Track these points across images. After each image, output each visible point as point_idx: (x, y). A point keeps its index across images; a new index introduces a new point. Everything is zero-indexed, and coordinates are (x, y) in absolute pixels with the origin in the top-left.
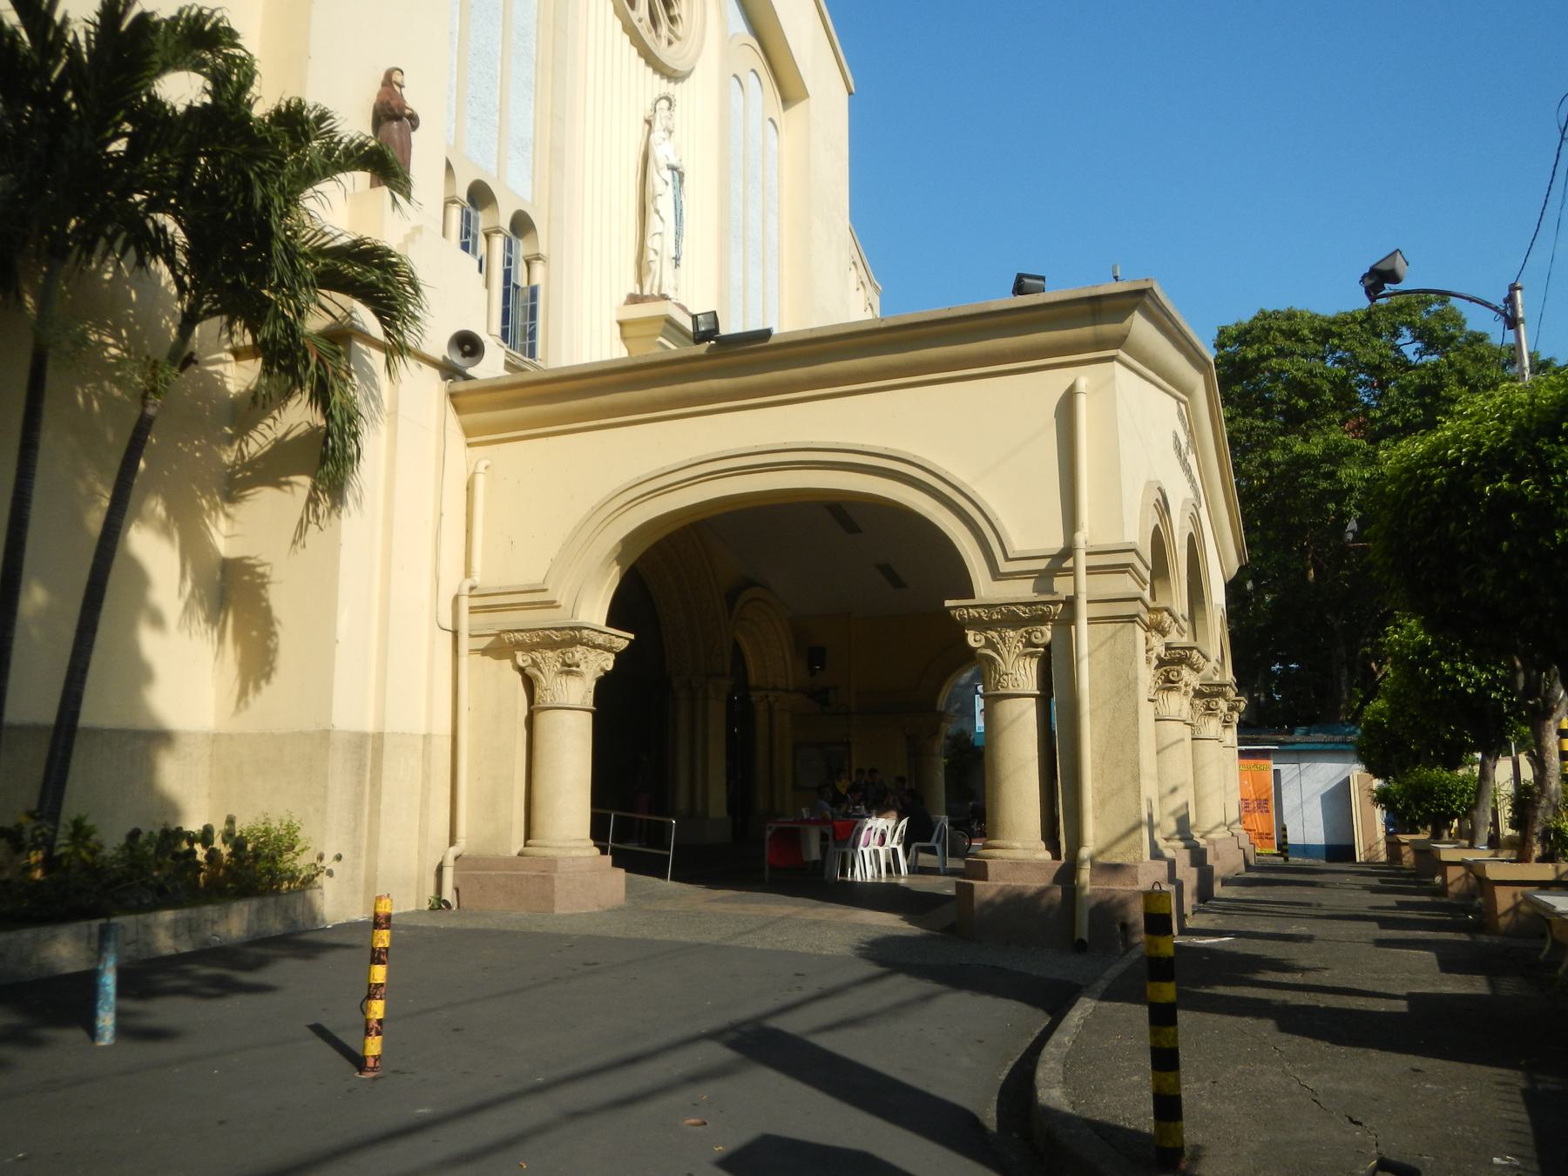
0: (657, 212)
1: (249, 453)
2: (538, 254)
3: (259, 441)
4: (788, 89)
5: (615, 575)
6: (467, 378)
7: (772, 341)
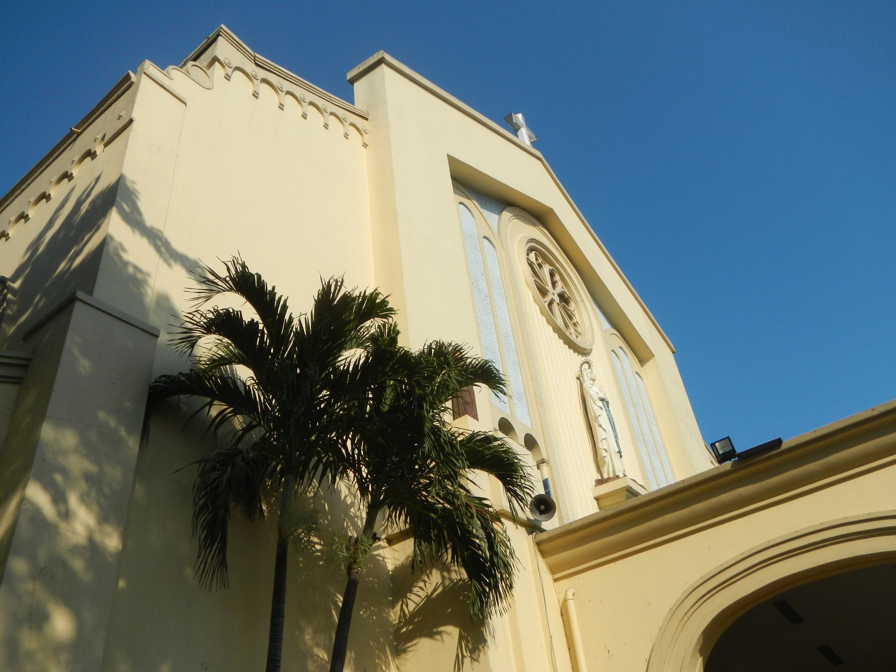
0: (600, 426)
2: (543, 459)
3: (415, 600)
4: (642, 355)
5: (700, 665)
6: (542, 531)
7: (784, 446)
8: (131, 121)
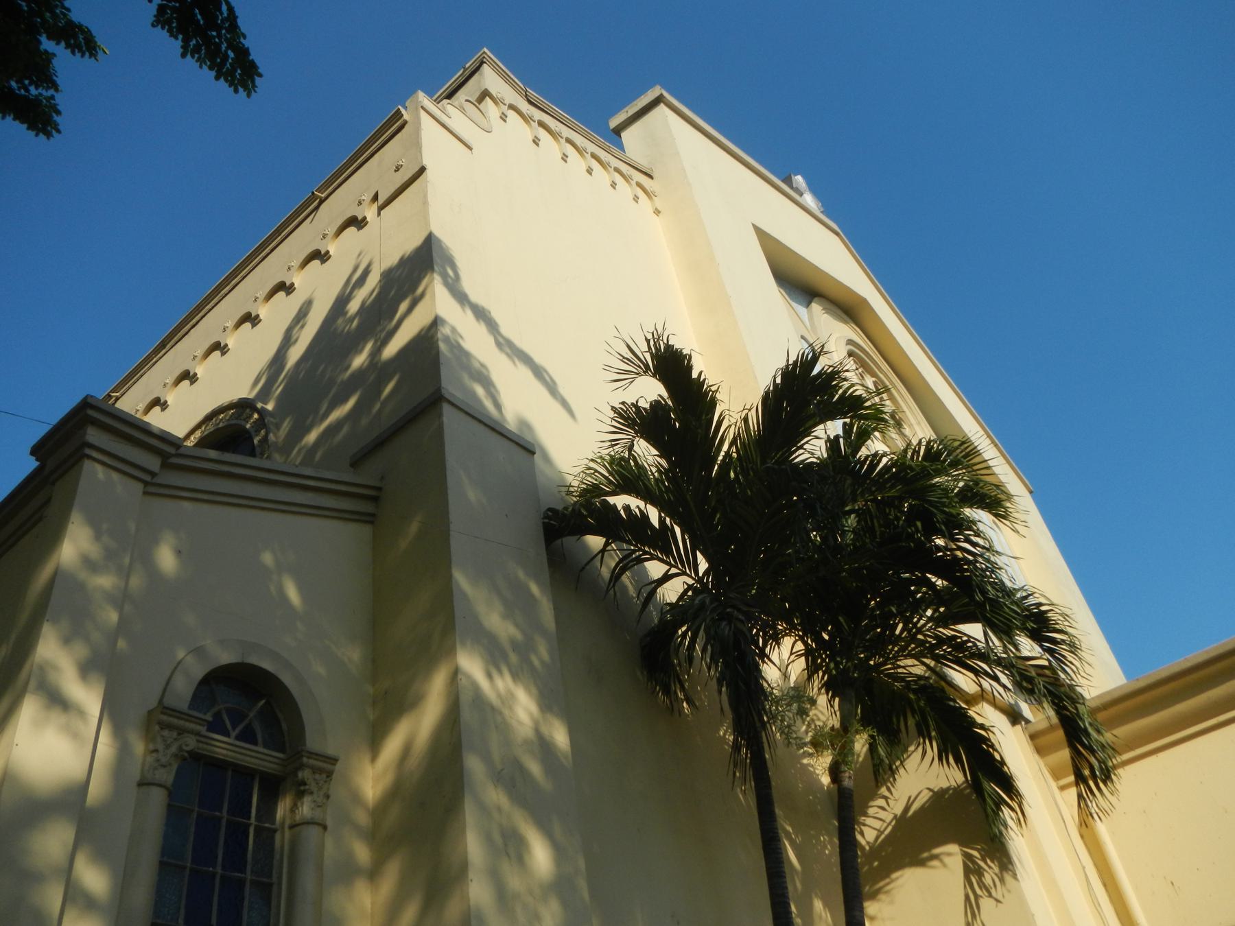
1: (868, 843)
8: (422, 170)
